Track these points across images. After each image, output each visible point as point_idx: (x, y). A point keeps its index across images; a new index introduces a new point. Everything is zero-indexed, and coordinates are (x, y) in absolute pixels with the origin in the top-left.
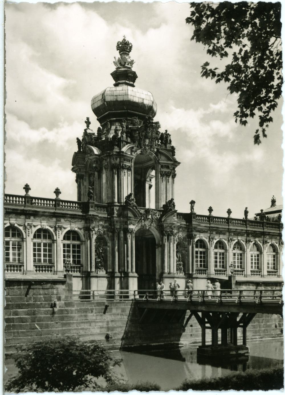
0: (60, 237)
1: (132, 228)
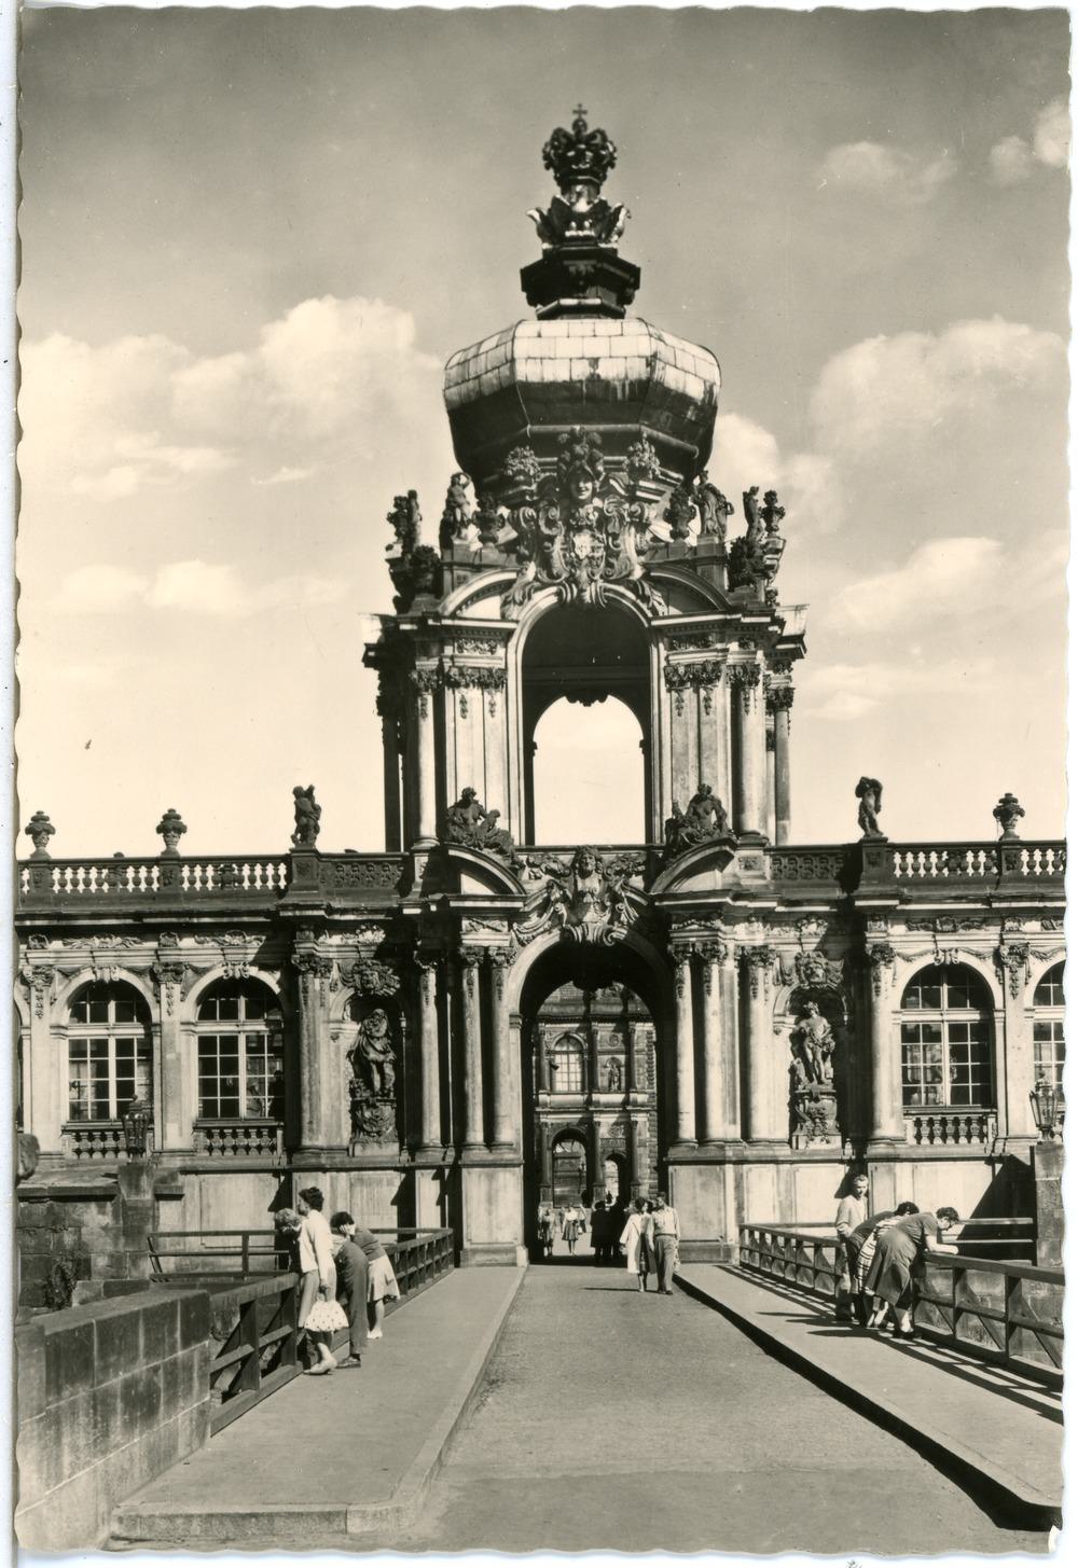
0: (177, 1010)
1: (486, 944)
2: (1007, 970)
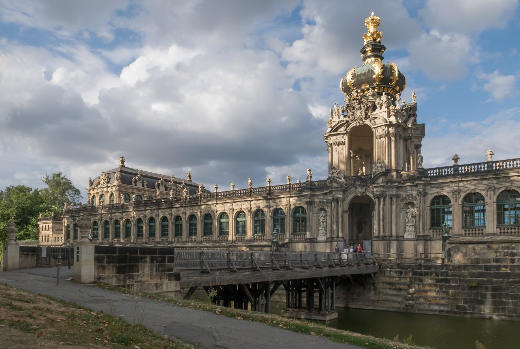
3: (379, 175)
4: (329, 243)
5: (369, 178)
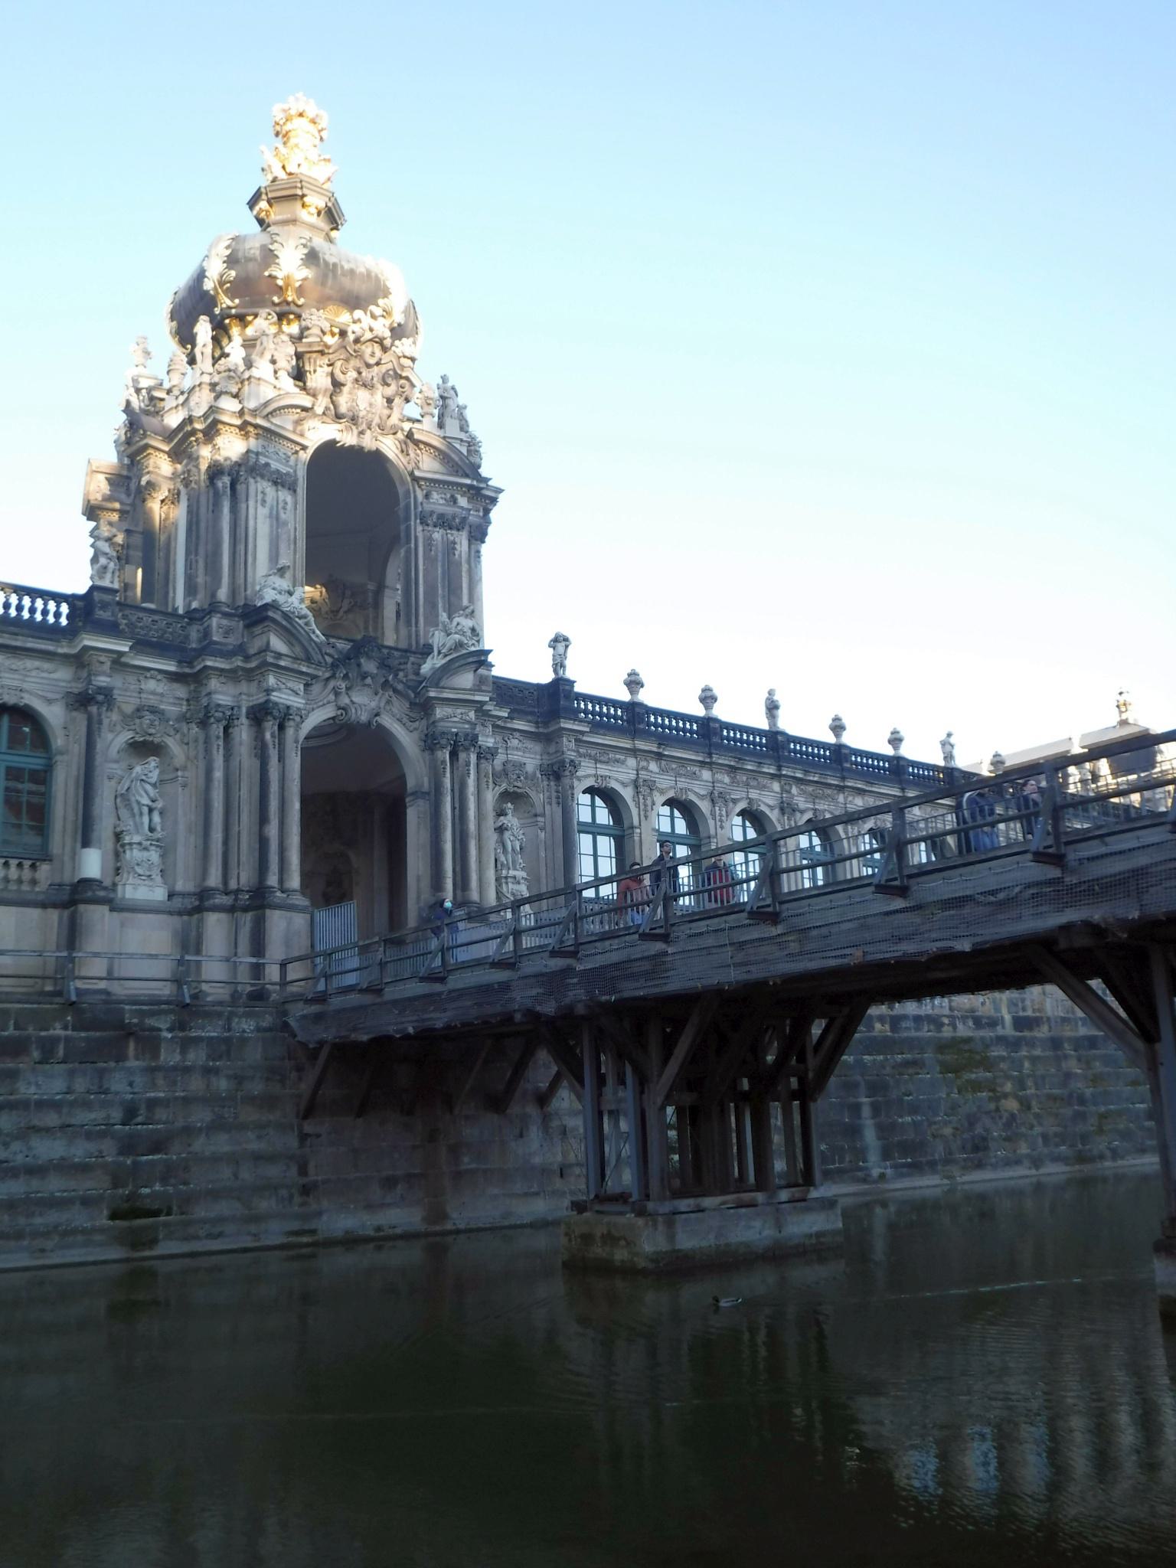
1: (289, 703)
2: (641, 797)
3: (471, 660)
4: (223, 916)
5: (397, 662)
